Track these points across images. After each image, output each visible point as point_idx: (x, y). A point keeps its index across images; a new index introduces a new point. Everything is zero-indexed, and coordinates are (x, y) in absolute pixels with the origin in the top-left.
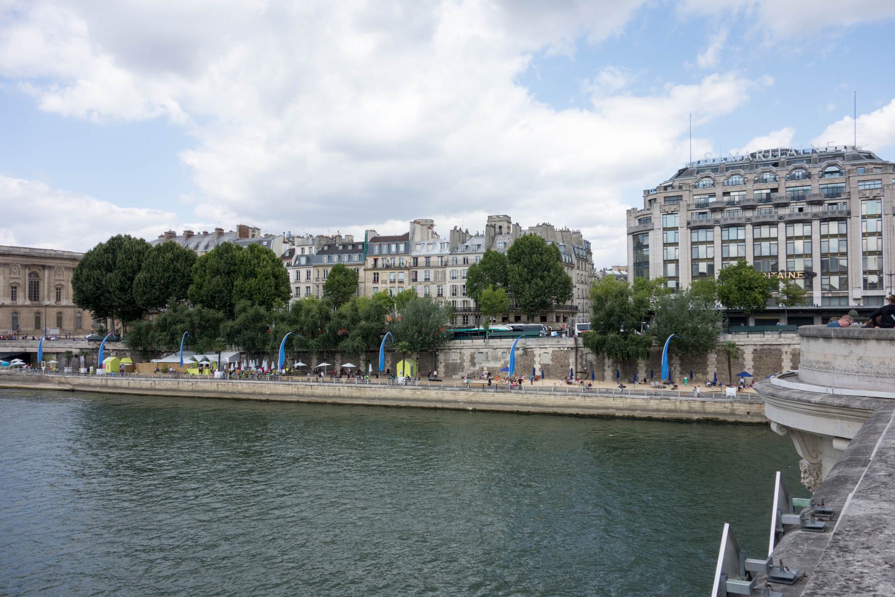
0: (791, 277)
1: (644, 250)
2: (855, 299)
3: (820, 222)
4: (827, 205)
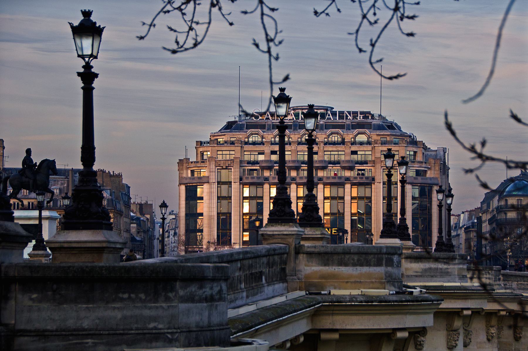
1: (198, 201)
3: (351, 186)
4: (357, 170)
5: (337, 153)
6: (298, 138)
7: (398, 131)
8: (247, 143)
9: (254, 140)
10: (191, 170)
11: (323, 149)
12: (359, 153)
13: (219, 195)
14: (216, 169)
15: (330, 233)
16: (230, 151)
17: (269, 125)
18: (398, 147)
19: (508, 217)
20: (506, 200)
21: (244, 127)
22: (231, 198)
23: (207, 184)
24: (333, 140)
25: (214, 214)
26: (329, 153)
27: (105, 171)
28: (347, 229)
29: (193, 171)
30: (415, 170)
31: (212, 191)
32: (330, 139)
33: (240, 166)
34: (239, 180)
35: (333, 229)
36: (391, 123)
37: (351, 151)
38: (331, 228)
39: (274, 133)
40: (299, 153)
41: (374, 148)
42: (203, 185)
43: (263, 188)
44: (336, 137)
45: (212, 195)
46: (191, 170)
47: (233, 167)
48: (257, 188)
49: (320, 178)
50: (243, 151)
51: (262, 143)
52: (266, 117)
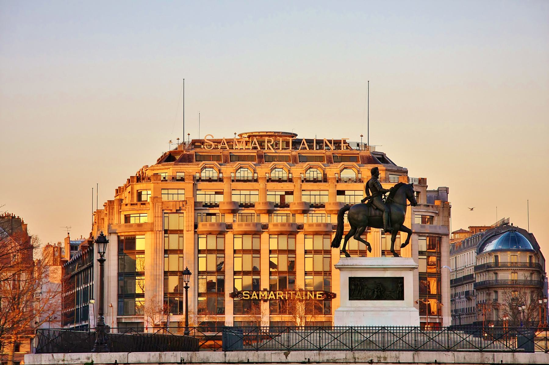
0: (310, 297)
5: (318, 193)
6: (266, 173)
7: (391, 165)
8: (200, 180)
9: (207, 175)
10: (125, 215)
11: (301, 187)
12: (346, 193)
15: (313, 297)
16: (168, 189)
17: (226, 156)
19: (499, 278)
20: (496, 257)
21: (193, 159)
22: (183, 252)
23: (150, 232)
24: (312, 176)
25: (160, 274)
26: (308, 193)
27: (15, 217)
28: (335, 293)
29: (128, 216)
30: (421, 216)
32: (238, 175)
33: (195, 210)
34: (193, 228)
35: (318, 292)
36: (382, 155)
37: (337, 191)
38: (315, 291)
39: (234, 167)
40: (268, 193)
43: (225, 238)
44: (315, 173)
46: (125, 215)
48: (217, 238)
50: (195, 189)
51: (221, 180)
52: (221, 145)
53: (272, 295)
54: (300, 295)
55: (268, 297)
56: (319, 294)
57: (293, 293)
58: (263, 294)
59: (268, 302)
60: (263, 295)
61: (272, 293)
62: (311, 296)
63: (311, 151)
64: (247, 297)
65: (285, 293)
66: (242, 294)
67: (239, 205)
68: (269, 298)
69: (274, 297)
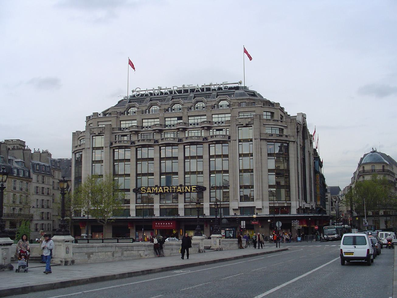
0: (187, 190)
2: (234, 210)
4: (215, 130)
11: (187, 114)
13: (94, 160)
14: (91, 137)
15: (189, 190)
18: (255, 108)
31: (87, 156)
34: (109, 145)
35: (193, 187)
36: (254, 93)
41: (233, 110)
42: (82, 152)
45: (87, 159)
47: (104, 133)
49: (180, 139)
53: (161, 190)
54: (180, 189)
55: (158, 191)
56: (193, 188)
57: (175, 188)
58: (155, 189)
59: (159, 195)
60: (155, 190)
61: (161, 188)
62: (187, 188)
63: (203, 93)
64: (144, 191)
65: (170, 188)
66: (141, 189)
67: (144, 128)
68: (159, 192)
69: (162, 191)
